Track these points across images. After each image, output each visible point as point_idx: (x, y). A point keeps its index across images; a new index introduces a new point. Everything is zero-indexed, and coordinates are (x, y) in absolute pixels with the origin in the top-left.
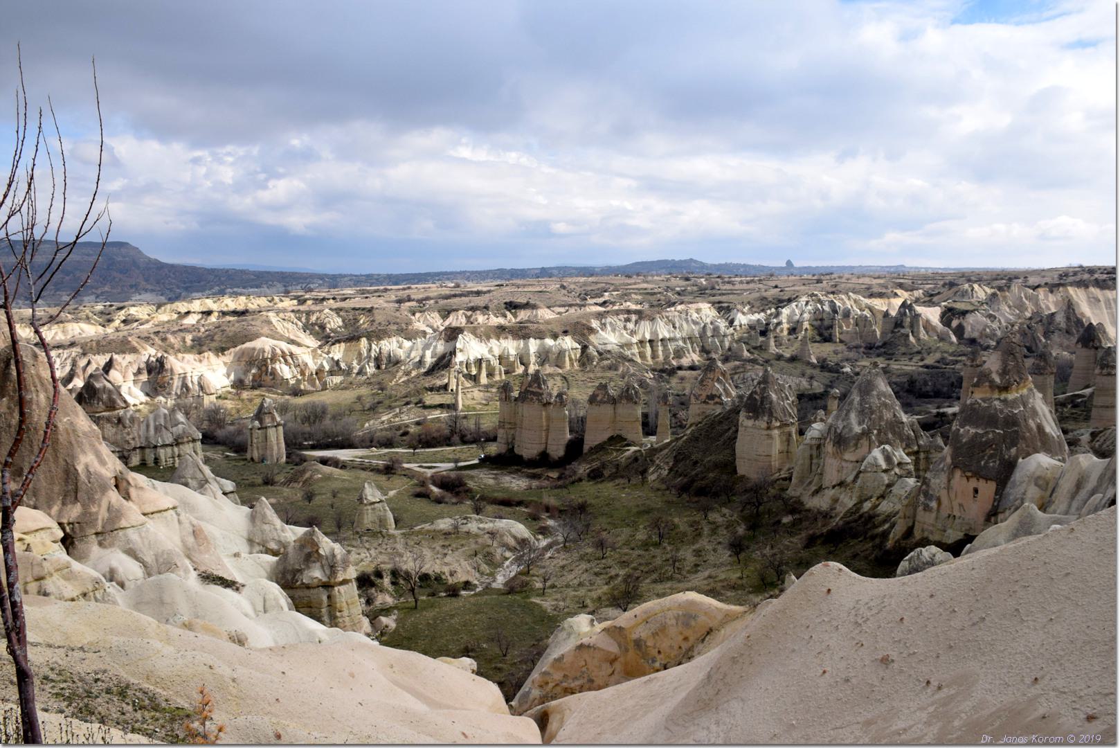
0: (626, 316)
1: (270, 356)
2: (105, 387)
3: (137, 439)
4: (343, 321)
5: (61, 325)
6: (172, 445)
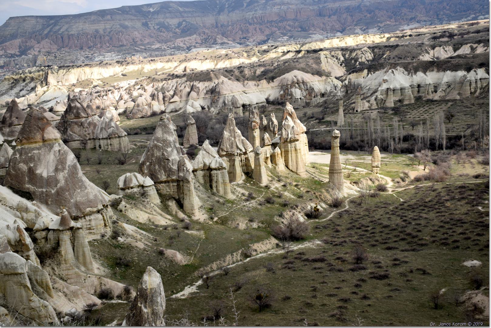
1: (290, 83)
2: (76, 106)
3: (91, 134)
4: (374, 56)
5: (230, 60)
6: (106, 139)
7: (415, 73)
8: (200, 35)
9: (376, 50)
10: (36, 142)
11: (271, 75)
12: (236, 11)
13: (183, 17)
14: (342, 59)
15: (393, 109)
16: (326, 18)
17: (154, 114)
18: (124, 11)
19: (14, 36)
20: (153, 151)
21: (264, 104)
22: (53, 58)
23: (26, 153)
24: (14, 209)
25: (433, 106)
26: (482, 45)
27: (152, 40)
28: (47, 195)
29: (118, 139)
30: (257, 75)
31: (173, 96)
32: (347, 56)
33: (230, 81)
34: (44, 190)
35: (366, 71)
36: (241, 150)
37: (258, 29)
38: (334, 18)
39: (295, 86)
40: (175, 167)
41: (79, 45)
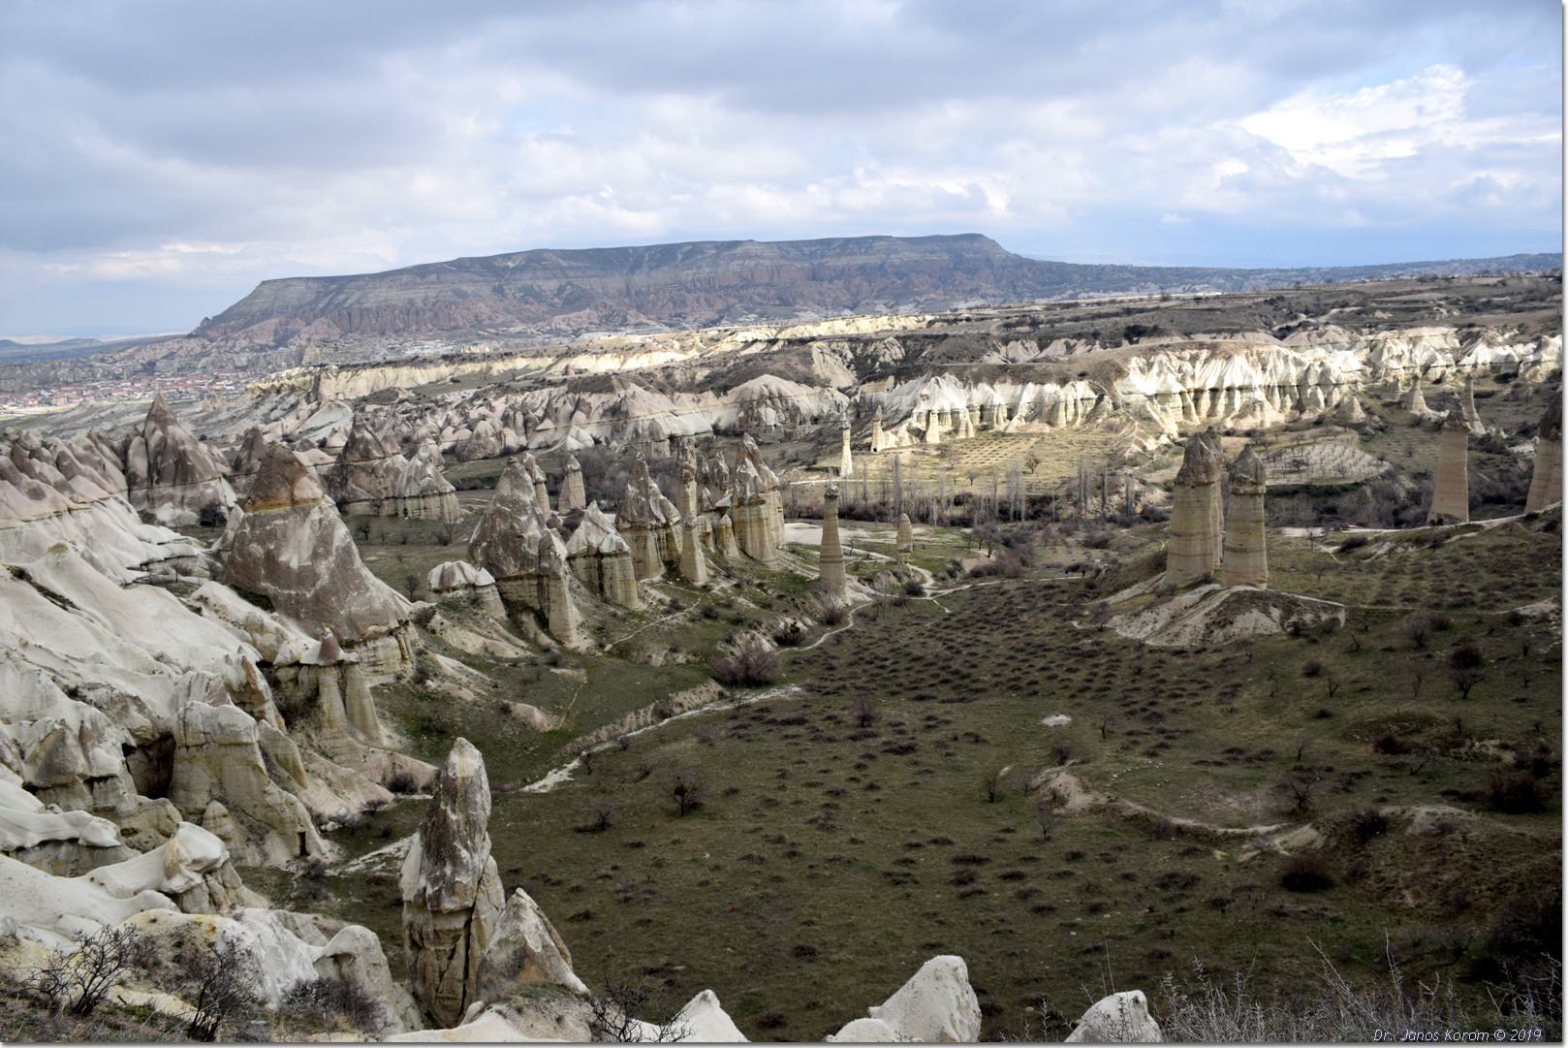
0: (1195, 352)
6: (417, 497)
7: (976, 384)
8: (597, 308)
9: (909, 343)
10: (279, 505)
11: (721, 382)
12: (666, 268)
13: (567, 277)
14: (850, 356)
15: (938, 448)
16: (825, 284)
17: (507, 452)
18: (461, 266)
19: (266, 314)
20: (494, 521)
22: (332, 351)
23: (262, 525)
24: (240, 626)
25: (1004, 444)
26: (1083, 341)
27: (510, 317)
28: (298, 602)
29: (437, 498)
31: (542, 420)
32: (859, 351)
33: (647, 393)
34: (293, 592)
35: (891, 379)
36: (658, 520)
37: (702, 300)
38: (839, 283)
40: (534, 552)
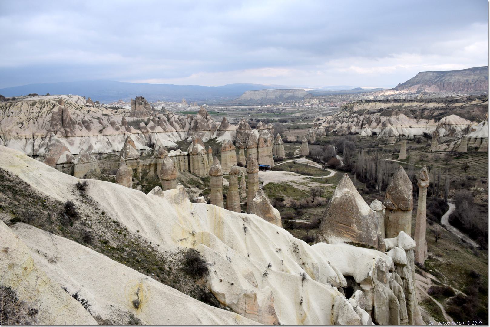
17: (351, 134)
19: (418, 83)
21: (421, 137)
30: (433, 115)
39: (442, 126)
41: (453, 89)
